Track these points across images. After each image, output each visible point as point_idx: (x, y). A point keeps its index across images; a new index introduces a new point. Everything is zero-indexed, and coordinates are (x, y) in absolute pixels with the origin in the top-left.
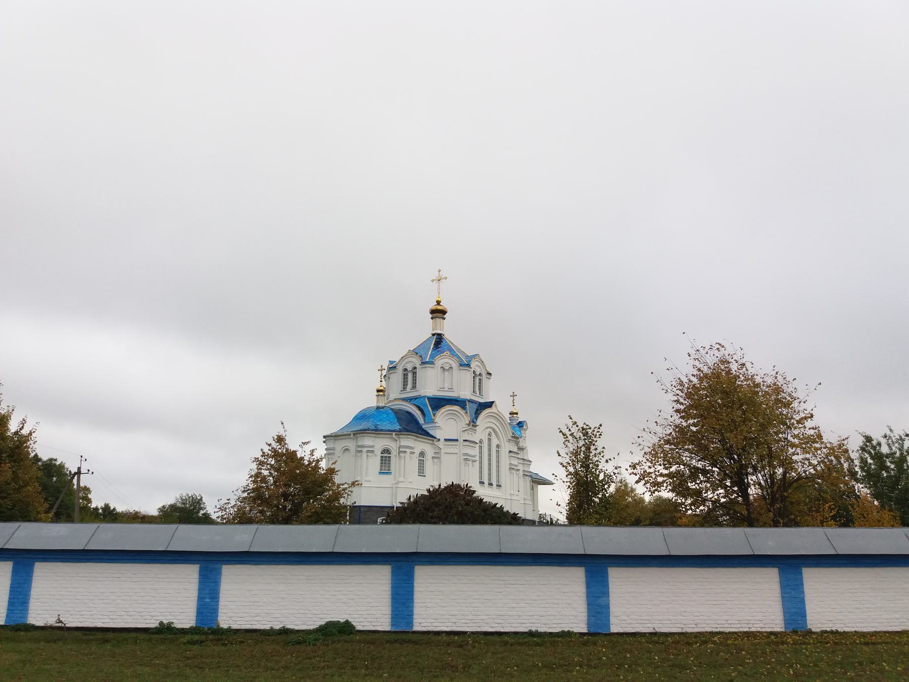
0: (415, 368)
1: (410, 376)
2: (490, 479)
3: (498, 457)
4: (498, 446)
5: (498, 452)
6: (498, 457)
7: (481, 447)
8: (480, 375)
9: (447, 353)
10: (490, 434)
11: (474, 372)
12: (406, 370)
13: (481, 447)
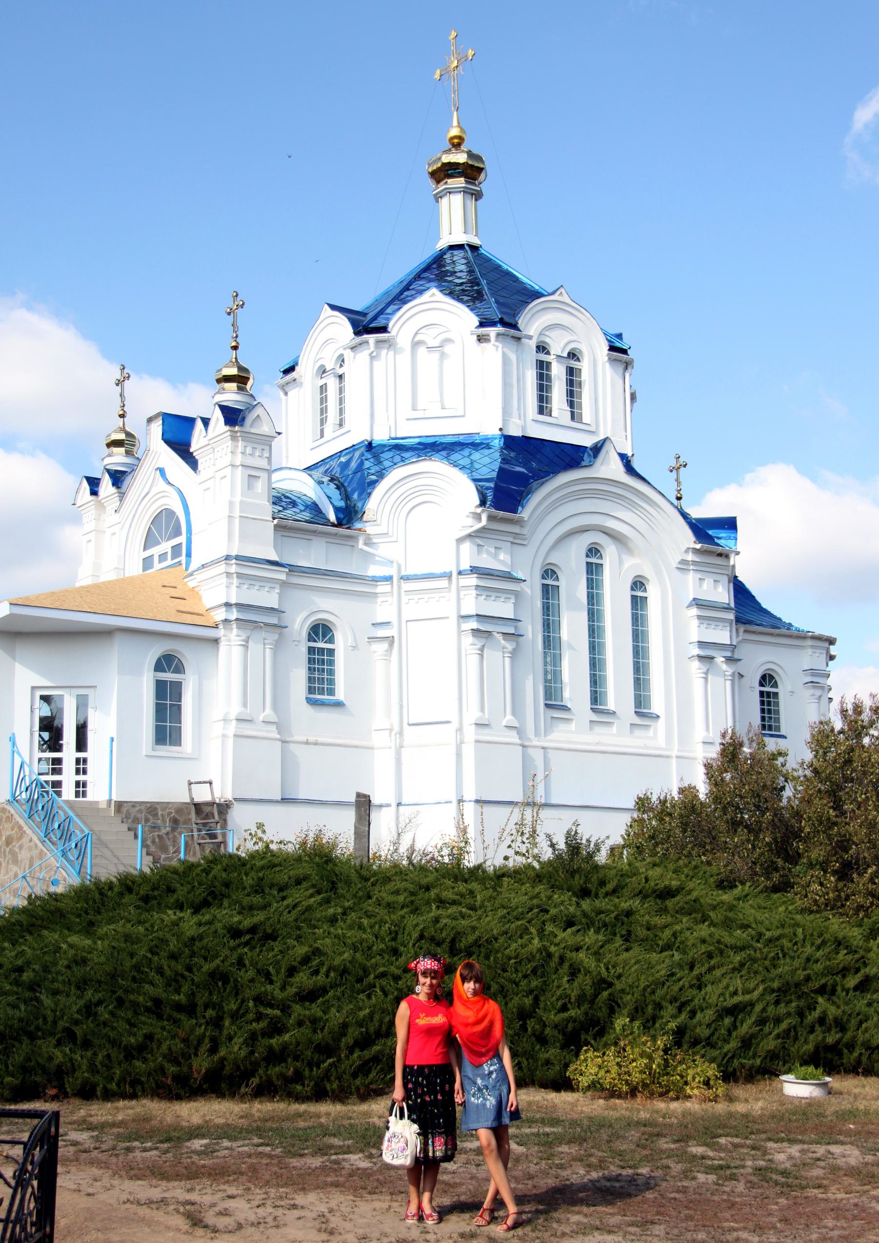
0: (341, 361)
1: (332, 383)
2: (596, 698)
3: (638, 619)
4: (638, 584)
5: (638, 603)
6: (638, 619)
7: (549, 592)
8: (573, 355)
9: (433, 295)
10: (593, 551)
11: (542, 348)
12: (323, 371)
13: (549, 592)
